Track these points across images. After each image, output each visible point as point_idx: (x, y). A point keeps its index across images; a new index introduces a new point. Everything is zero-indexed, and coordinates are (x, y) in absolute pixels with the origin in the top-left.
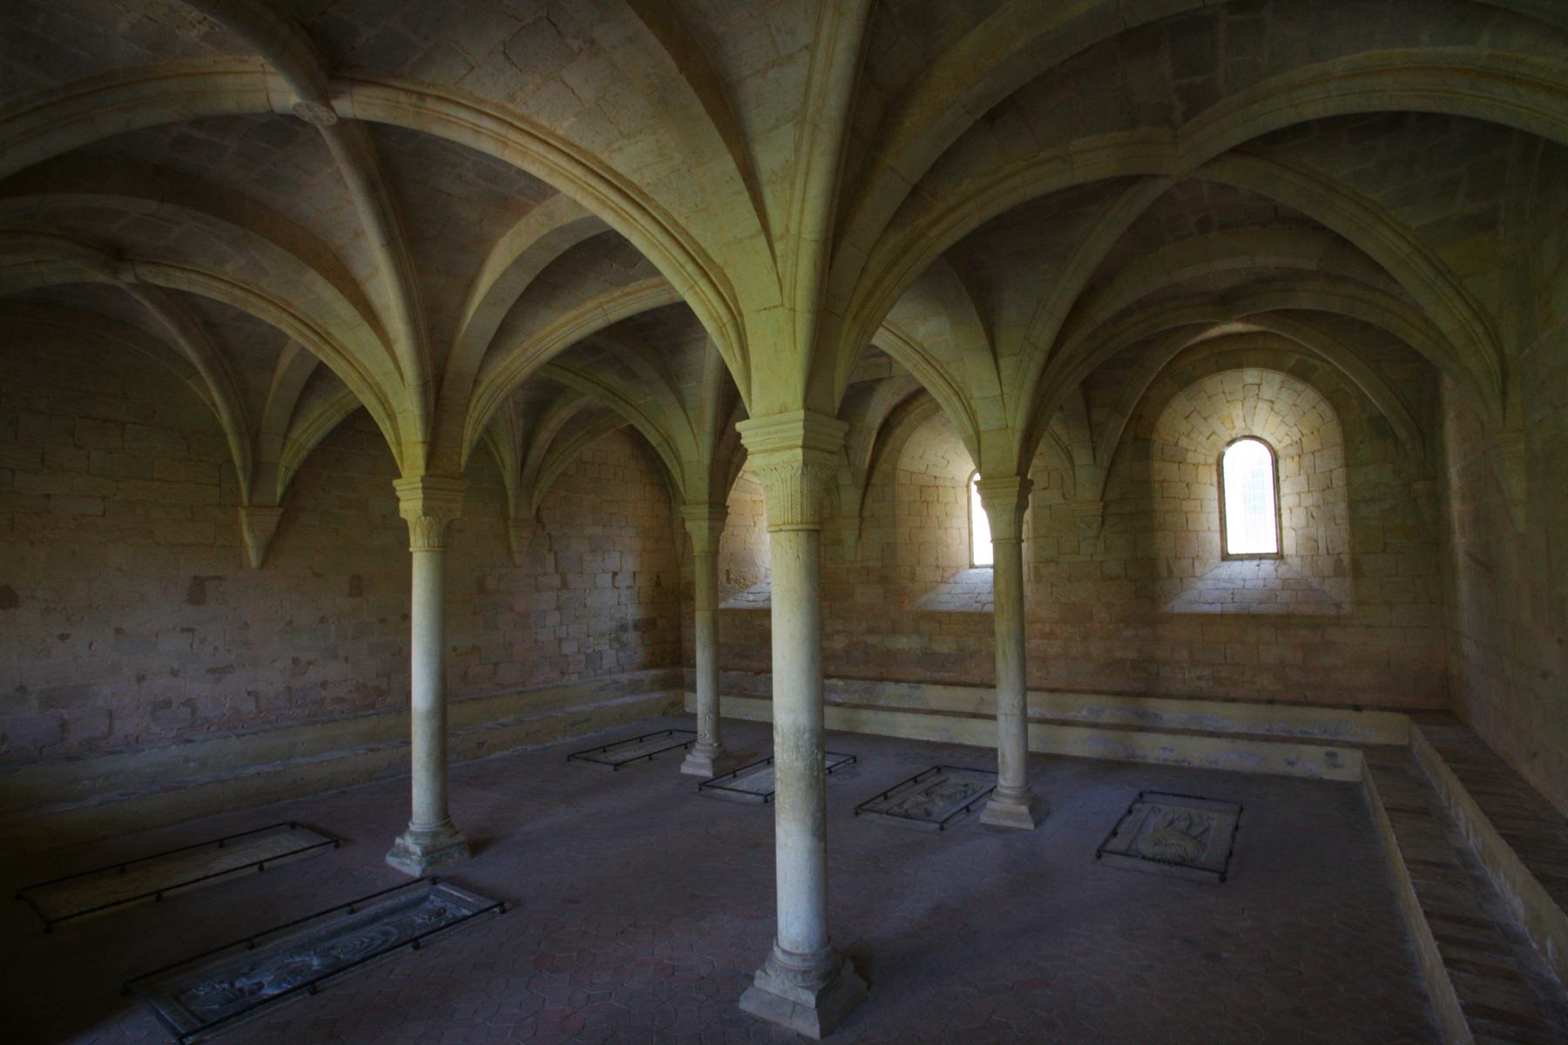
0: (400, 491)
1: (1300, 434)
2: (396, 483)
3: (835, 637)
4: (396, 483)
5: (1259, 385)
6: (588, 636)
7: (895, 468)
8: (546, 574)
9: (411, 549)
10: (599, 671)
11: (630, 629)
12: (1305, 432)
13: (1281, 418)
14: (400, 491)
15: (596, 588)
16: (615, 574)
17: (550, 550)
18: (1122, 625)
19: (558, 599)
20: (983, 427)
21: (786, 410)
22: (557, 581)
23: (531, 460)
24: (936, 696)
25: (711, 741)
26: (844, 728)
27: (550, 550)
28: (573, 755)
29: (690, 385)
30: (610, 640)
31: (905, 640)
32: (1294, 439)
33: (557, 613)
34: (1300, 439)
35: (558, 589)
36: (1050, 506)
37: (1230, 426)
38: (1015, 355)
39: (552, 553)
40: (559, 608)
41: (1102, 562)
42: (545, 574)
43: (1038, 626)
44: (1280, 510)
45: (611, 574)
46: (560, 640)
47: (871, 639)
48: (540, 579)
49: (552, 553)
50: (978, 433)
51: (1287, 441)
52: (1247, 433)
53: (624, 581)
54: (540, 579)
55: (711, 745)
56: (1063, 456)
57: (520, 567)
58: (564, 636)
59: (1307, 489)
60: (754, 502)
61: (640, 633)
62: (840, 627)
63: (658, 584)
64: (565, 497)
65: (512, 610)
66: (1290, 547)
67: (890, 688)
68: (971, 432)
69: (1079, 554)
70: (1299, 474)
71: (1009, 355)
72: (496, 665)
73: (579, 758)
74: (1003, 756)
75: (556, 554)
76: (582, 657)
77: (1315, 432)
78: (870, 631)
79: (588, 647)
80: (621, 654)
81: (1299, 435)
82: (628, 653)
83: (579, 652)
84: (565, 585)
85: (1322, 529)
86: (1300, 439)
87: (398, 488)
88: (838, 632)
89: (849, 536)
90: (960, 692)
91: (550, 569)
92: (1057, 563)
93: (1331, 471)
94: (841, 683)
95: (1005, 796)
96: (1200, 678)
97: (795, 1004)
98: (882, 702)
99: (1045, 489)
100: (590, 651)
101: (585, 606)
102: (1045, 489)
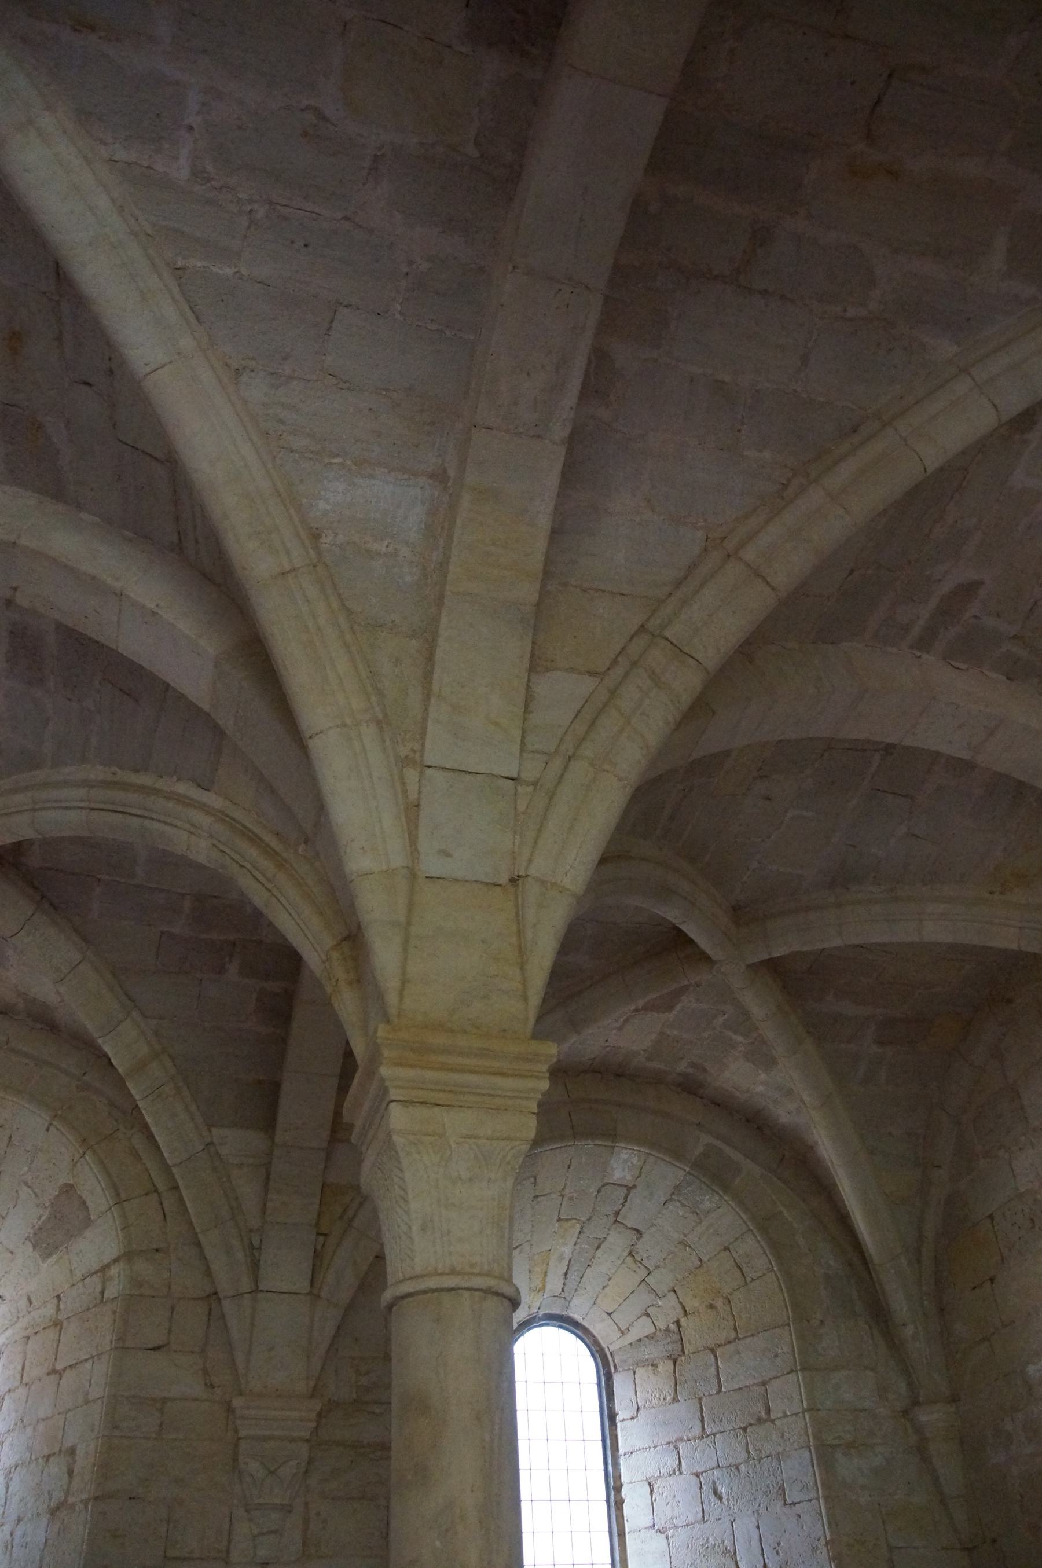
1: (679, 1310)
5: (630, 1189)
12: (691, 1304)
13: (643, 1273)
32: (661, 1325)
34: (678, 1323)
36: (165, 1400)
37: (537, 1282)
38: (592, 673)
44: (618, 1489)
50: (412, 875)
51: (642, 1328)
52: (556, 1311)
56: (240, 1255)
59: (697, 1431)
68: (398, 861)
70: (675, 1400)
71: (572, 670)
77: (719, 1303)
85: (745, 1525)
86: (678, 1323)
93: (764, 1384)
99: (154, 1349)
102: (154, 1349)
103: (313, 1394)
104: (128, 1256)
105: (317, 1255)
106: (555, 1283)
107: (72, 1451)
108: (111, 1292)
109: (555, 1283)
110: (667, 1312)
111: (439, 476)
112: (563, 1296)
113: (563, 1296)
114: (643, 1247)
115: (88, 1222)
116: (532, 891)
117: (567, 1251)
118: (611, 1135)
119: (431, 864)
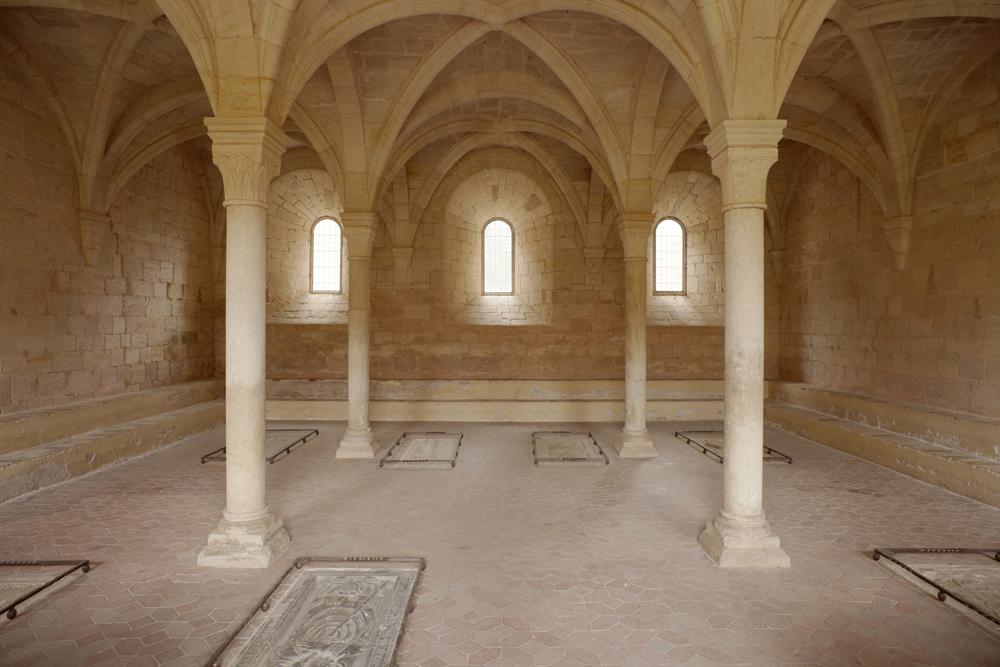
0: (213, 131)
2: (207, 121)
3: (384, 347)
4: (207, 121)
6: (148, 345)
7: (443, 211)
8: (113, 277)
9: (225, 204)
10: (156, 382)
11: (180, 341)
14: (213, 131)
15: (154, 297)
16: (169, 285)
17: (117, 253)
18: (611, 334)
19: (124, 306)
20: (632, 176)
21: (764, 118)
22: (123, 287)
23: (113, 149)
24: (483, 388)
25: (365, 427)
26: (410, 419)
27: (117, 253)
28: (206, 456)
29: (377, 100)
30: (164, 350)
31: (447, 348)
33: (123, 319)
35: (124, 295)
39: (119, 256)
40: (124, 315)
41: (599, 291)
42: (113, 277)
43: (554, 335)
45: (165, 285)
46: (125, 348)
47: (417, 348)
48: (108, 281)
49: (119, 256)
53: (176, 293)
54: (108, 281)
55: (366, 430)
57: (91, 266)
58: (128, 345)
60: (289, 230)
61: (186, 345)
62: (389, 339)
63: (200, 300)
64: (131, 197)
65: (82, 313)
66: (692, 287)
67: (442, 385)
68: (626, 178)
69: (584, 284)
72: (68, 373)
73: (212, 459)
74: (633, 409)
75: (122, 257)
76: (142, 367)
78: (418, 341)
79: (147, 358)
80: (172, 365)
81: (707, 219)
82: (178, 365)
83: (140, 362)
84: (129, 291)
87: (209, 128)
88: (387, 343)
89: (401, 262)
90: (502, 385)
91: (118, 273)
92: (569, 290)
94: (398, 384)
95: (638, 437)
96: (657, 367)
97: (765, 550)
98: (435, 398)
100: (148, 361)
101: (146, 315)
103: (603, 248)
104: (553, 214)
105: (603, 213)
106: (671, 208)
107: (545, 261)
108: (550, 222)
109: (671, 208)
110: (704, 218)
111: (634, 85)
112: (674, 212)
113: (674, 212)
114: (698, 200)
115: (540, 204)
116: (653, 181)
117: (675, 201)
118: (689, 169)
119: (632, 176)
